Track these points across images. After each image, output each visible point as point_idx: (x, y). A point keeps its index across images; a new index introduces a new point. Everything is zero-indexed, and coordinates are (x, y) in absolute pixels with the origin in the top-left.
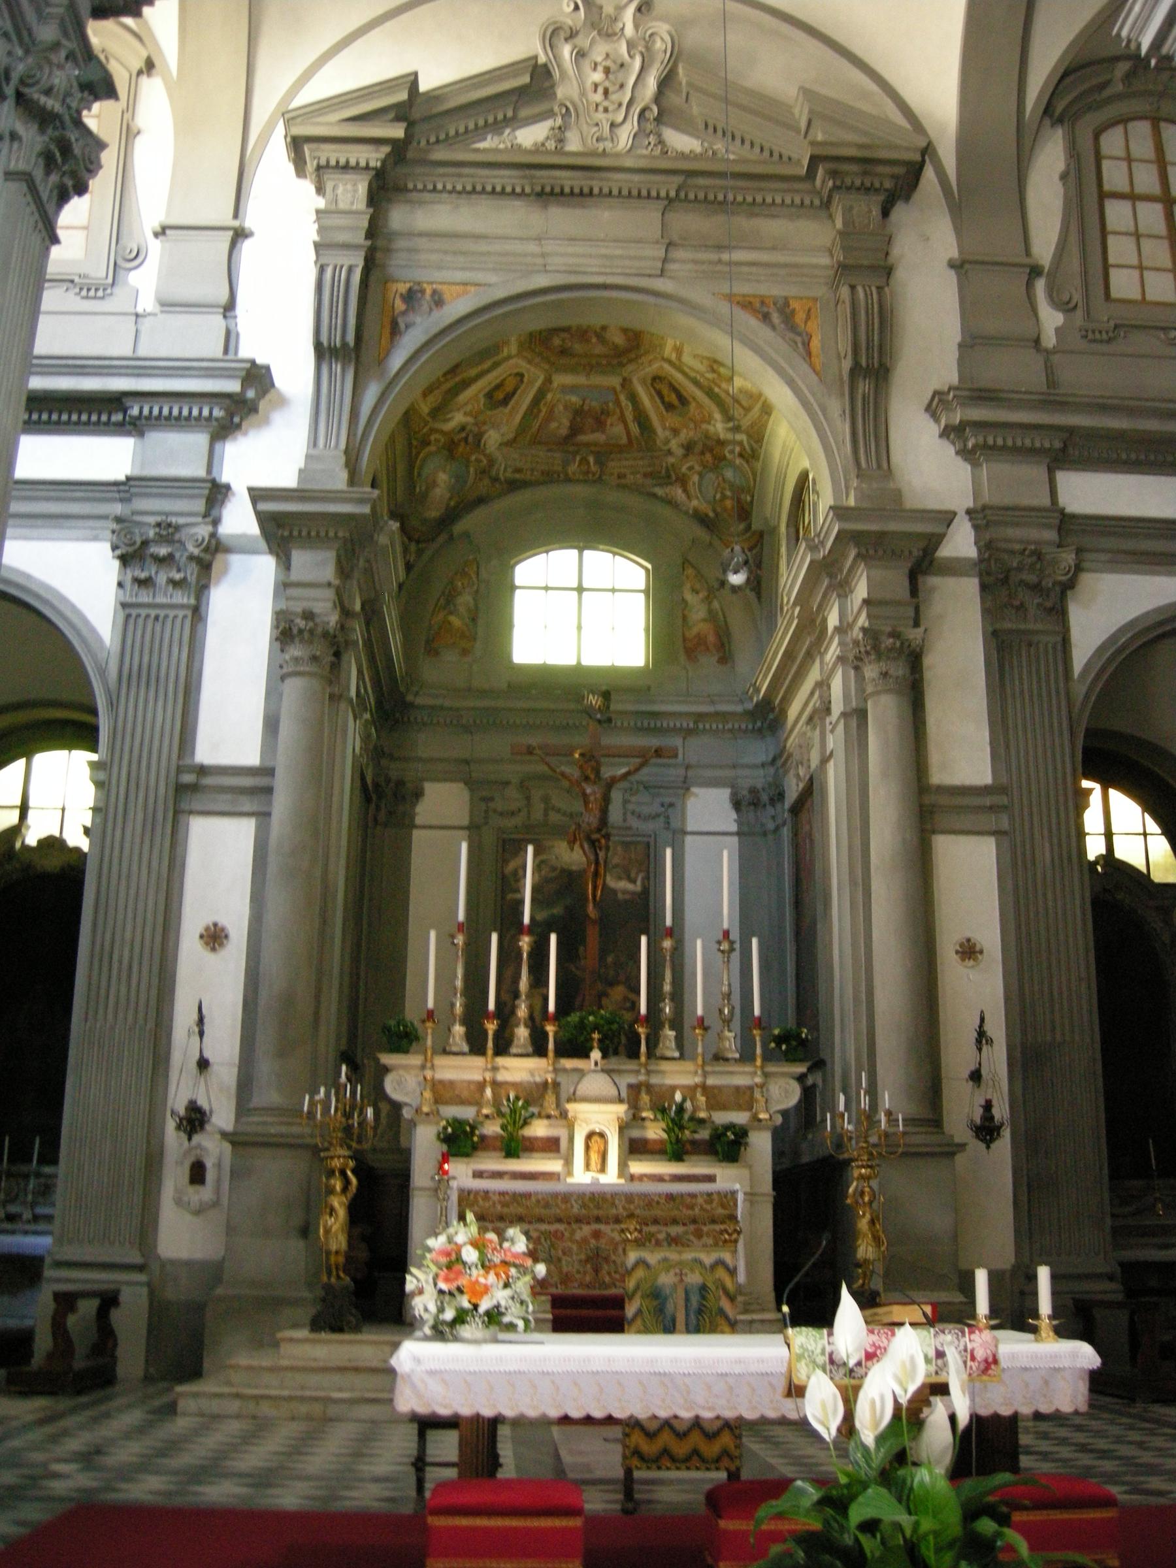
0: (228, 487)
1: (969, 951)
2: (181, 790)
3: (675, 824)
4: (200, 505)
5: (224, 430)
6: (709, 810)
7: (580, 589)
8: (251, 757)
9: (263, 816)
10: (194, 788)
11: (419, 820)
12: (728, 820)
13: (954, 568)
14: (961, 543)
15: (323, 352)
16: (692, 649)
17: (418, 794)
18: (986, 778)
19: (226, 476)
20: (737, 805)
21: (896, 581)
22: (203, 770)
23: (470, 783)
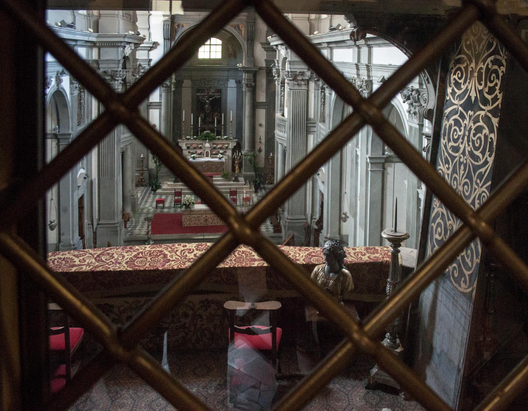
0: (152, 60)
1: (261, 125)
2: (148, 106)
3: (226, 86)
4: (147, 63)
5: (149, 50)
6: (232, 83)
7: (210, 45)
8: (158, 101)
9: (160, 109)
10: (150, 105)
11: (183, 86)
12: (235, 85)
13: (261, 68)
14: (264, 65)
15: (164, 39)
16: (230, 56)
17: (183, 82)
18: (265, 101)
19: (150, 58)
20: (236, 82)
21: (251, 75)
22: (151, 103)
23: (192, 80)
